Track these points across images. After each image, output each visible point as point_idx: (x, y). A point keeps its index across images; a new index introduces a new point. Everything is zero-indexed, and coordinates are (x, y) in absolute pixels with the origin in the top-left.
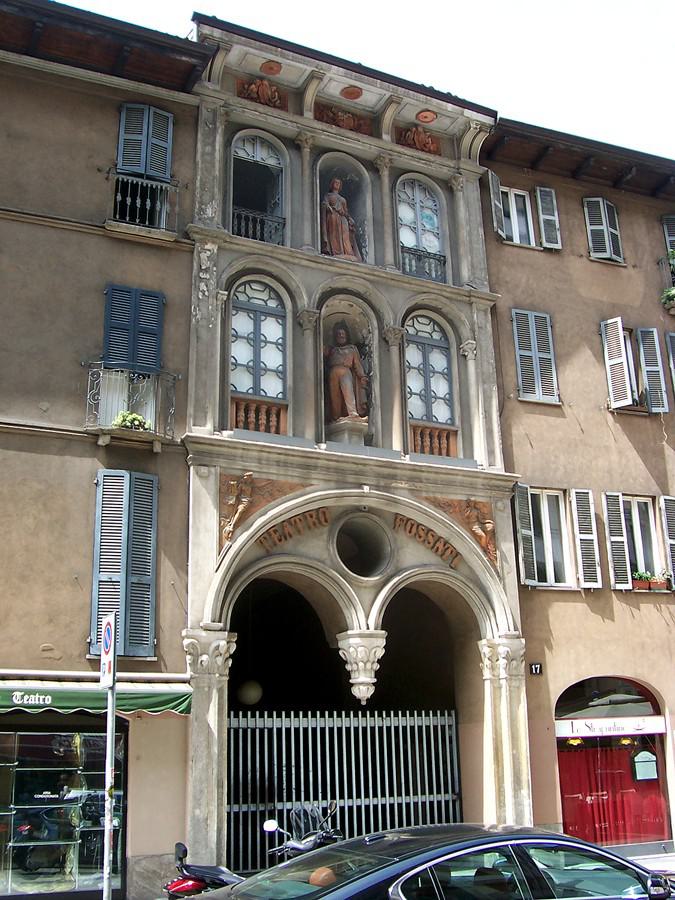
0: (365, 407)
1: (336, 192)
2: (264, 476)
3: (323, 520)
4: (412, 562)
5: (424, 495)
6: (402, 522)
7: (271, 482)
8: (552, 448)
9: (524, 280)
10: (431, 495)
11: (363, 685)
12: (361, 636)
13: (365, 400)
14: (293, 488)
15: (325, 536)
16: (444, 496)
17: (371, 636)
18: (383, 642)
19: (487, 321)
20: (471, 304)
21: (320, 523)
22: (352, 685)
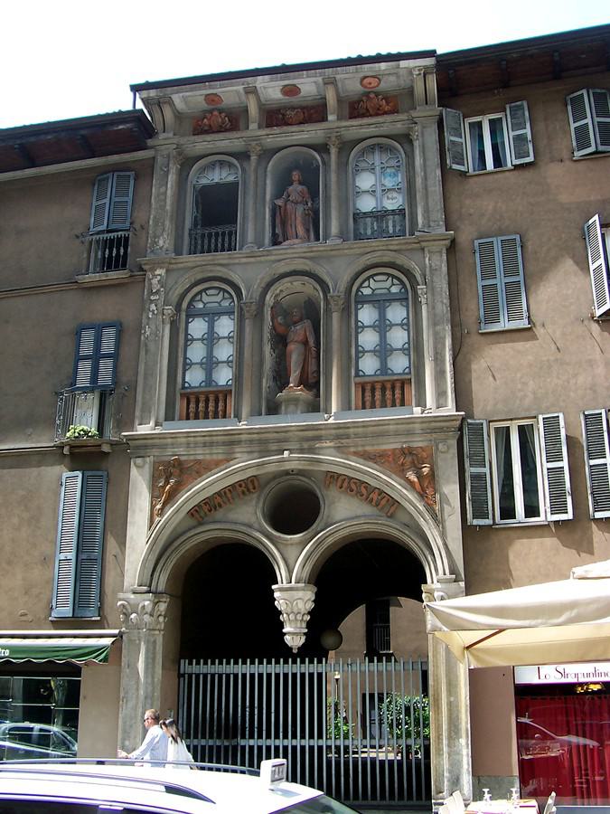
2: (192, 458)
3: (251, 487)
4: (344, 517)
5: (352, 450)
6: (333, 478)
7: (199, 462)
8: (519, 375)
9: (490, 207)
10: (360, 449)
11: (294, 635)
12: (281, 590)
14: (217, 464)
16: (376, 448)
19: (441, 262)
21: (248, 490)
22: (285, 634)
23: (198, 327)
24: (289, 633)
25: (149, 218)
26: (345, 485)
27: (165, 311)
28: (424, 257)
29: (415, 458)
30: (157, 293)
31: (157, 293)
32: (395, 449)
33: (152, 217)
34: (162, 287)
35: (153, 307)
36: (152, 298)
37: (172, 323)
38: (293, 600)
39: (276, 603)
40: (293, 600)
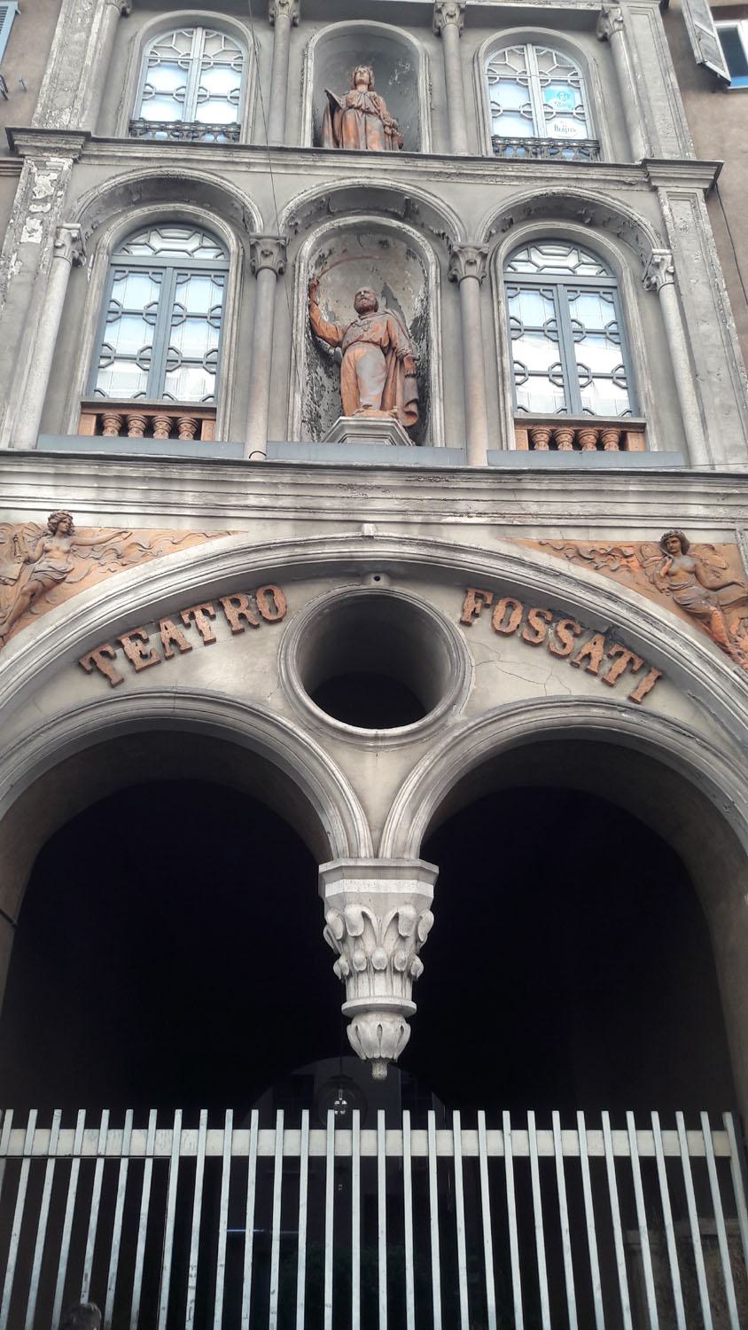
0: (413, 408)
1: (363, 88)
10: (555, 535)
11: (379, 1010)
13: (415, 396)
15: (271, 646)
17: (379, 871)
18: (429, 891)
19: (698, 217)
20: (655, 189)
23: (136, 292)
24: (366, 1010)
25: (44, 72)
26: (516, 617)
27: (64, 231)
28: (660, 206)
29: (698, 563)
30: (44, 200)
31: (44, 200)
32: (647, 544)
33: (49, 71)
34: (61, 189)
35: (34, 223)
36: (33, 208)
37: (76, 263)
38: (378, 915)
39: (330, 917)
40: (378, 915)
